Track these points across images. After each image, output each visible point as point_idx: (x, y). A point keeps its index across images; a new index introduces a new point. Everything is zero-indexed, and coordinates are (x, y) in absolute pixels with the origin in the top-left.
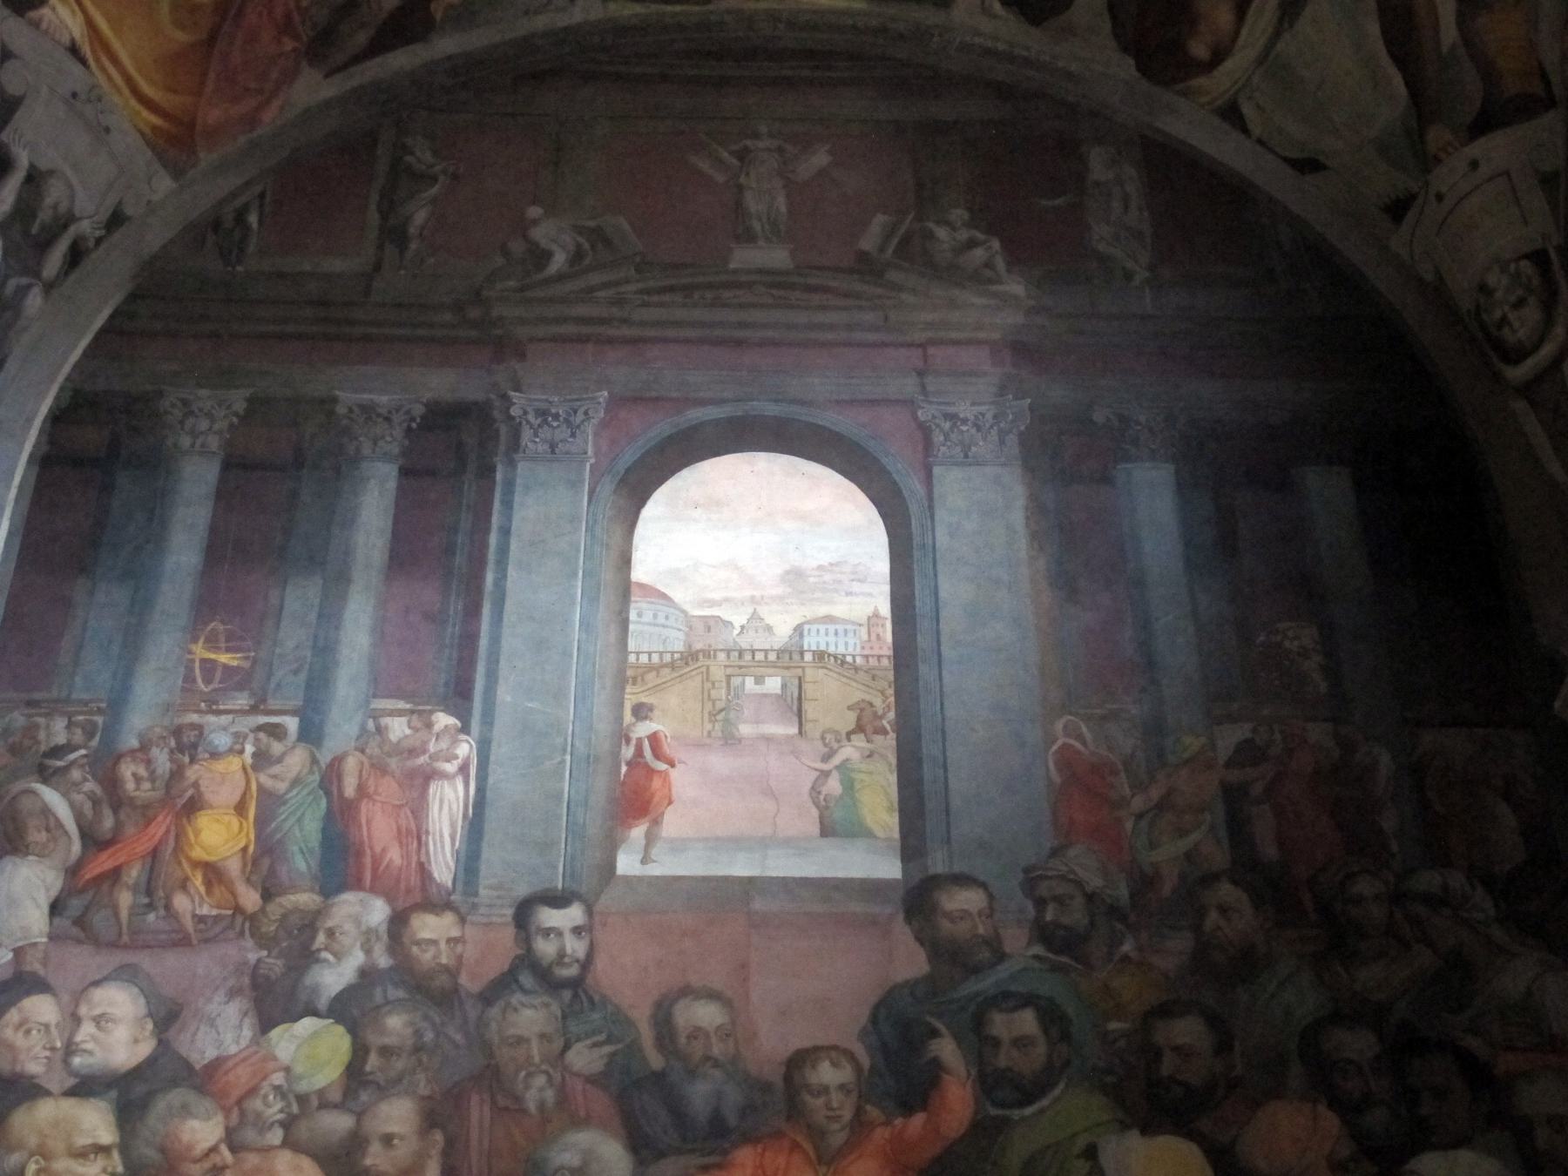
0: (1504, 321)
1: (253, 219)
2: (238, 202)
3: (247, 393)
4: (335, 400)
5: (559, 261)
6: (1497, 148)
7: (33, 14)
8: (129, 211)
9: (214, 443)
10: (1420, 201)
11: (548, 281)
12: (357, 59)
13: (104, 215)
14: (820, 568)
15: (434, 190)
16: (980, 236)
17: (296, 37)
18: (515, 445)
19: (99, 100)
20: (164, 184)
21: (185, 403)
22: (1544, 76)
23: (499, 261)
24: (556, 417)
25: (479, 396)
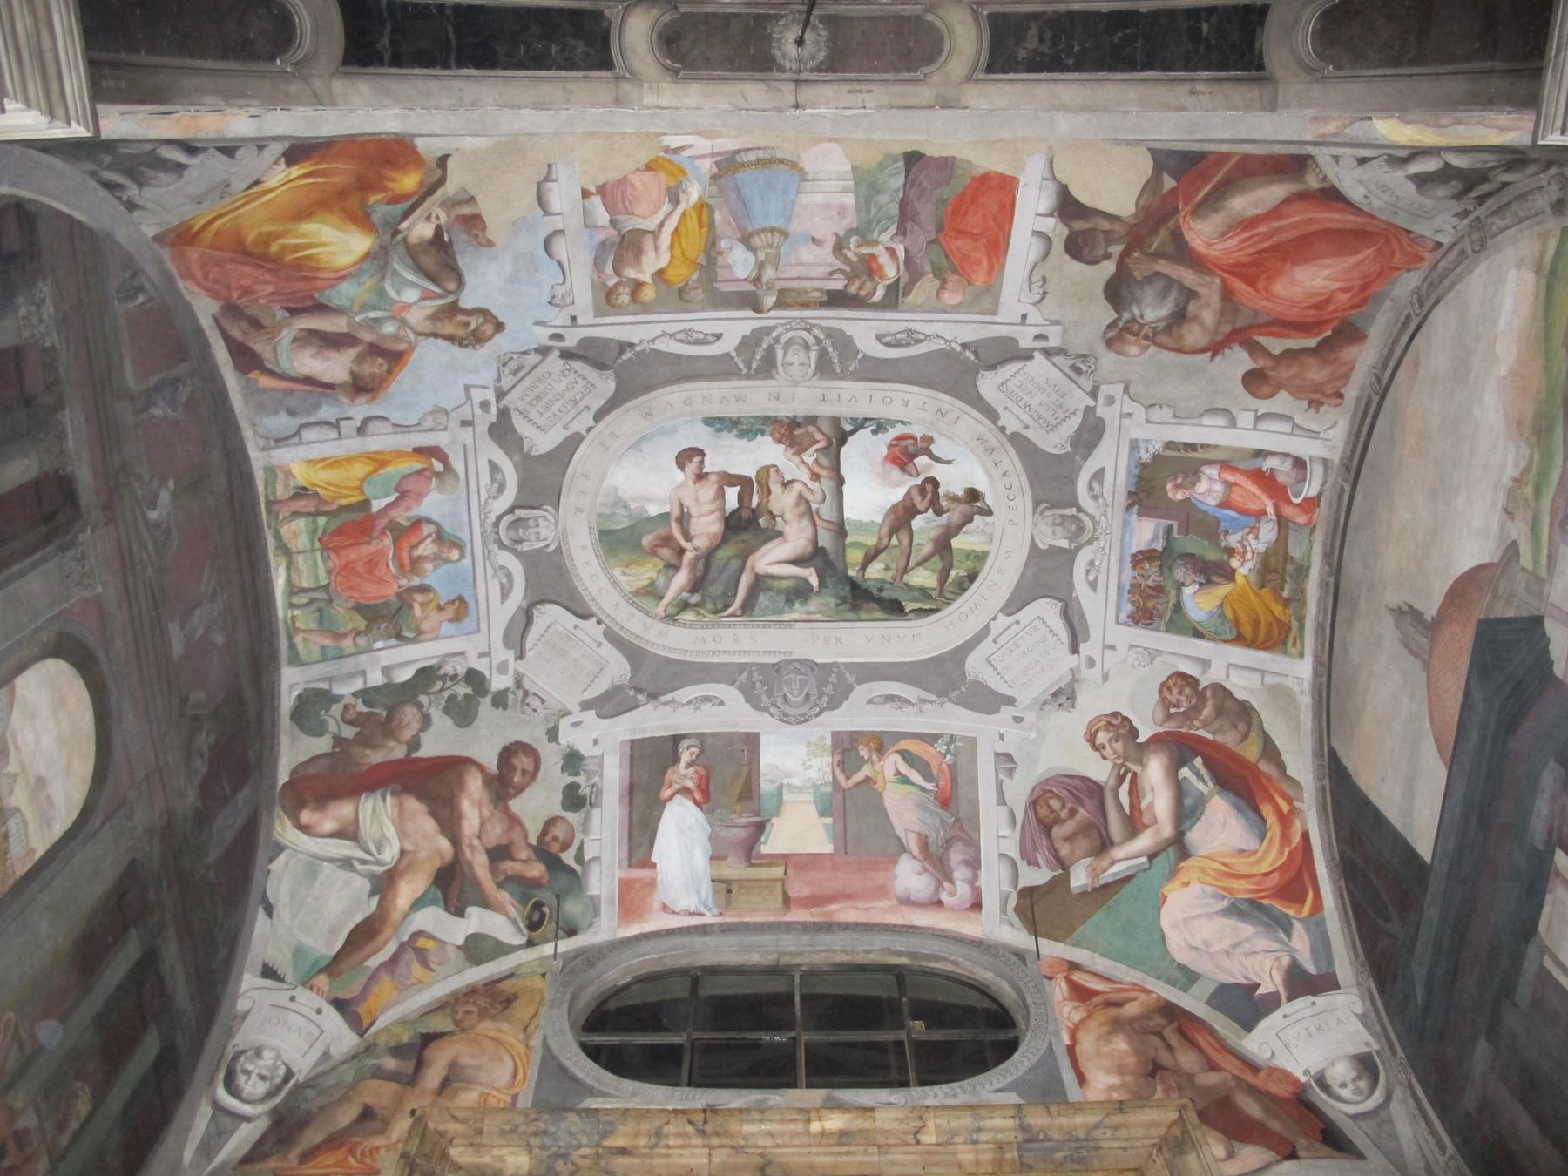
0: (247, 1073)
1: (141, 299)
2: (147, 286)
3: (57, 344)
4: (63, 409)
5: (153, 515)
6: (333, 1018)
7: (283, 160)
8: (136, 214)
9: (26, 334)
10: (285, 986)
11: (144, 514)
12: (220, 327)
13: (138, 200)
14: (48, 797)
15: (170, 412)
16: (206, 758)
17: (240, 297)
18: (63, 549)
19: (222, 198)
20: (150, 230)
21: (43, 300)
22: (372, 1024)
23: (147, 478)
24: (83, 567)
25: (83, 510)
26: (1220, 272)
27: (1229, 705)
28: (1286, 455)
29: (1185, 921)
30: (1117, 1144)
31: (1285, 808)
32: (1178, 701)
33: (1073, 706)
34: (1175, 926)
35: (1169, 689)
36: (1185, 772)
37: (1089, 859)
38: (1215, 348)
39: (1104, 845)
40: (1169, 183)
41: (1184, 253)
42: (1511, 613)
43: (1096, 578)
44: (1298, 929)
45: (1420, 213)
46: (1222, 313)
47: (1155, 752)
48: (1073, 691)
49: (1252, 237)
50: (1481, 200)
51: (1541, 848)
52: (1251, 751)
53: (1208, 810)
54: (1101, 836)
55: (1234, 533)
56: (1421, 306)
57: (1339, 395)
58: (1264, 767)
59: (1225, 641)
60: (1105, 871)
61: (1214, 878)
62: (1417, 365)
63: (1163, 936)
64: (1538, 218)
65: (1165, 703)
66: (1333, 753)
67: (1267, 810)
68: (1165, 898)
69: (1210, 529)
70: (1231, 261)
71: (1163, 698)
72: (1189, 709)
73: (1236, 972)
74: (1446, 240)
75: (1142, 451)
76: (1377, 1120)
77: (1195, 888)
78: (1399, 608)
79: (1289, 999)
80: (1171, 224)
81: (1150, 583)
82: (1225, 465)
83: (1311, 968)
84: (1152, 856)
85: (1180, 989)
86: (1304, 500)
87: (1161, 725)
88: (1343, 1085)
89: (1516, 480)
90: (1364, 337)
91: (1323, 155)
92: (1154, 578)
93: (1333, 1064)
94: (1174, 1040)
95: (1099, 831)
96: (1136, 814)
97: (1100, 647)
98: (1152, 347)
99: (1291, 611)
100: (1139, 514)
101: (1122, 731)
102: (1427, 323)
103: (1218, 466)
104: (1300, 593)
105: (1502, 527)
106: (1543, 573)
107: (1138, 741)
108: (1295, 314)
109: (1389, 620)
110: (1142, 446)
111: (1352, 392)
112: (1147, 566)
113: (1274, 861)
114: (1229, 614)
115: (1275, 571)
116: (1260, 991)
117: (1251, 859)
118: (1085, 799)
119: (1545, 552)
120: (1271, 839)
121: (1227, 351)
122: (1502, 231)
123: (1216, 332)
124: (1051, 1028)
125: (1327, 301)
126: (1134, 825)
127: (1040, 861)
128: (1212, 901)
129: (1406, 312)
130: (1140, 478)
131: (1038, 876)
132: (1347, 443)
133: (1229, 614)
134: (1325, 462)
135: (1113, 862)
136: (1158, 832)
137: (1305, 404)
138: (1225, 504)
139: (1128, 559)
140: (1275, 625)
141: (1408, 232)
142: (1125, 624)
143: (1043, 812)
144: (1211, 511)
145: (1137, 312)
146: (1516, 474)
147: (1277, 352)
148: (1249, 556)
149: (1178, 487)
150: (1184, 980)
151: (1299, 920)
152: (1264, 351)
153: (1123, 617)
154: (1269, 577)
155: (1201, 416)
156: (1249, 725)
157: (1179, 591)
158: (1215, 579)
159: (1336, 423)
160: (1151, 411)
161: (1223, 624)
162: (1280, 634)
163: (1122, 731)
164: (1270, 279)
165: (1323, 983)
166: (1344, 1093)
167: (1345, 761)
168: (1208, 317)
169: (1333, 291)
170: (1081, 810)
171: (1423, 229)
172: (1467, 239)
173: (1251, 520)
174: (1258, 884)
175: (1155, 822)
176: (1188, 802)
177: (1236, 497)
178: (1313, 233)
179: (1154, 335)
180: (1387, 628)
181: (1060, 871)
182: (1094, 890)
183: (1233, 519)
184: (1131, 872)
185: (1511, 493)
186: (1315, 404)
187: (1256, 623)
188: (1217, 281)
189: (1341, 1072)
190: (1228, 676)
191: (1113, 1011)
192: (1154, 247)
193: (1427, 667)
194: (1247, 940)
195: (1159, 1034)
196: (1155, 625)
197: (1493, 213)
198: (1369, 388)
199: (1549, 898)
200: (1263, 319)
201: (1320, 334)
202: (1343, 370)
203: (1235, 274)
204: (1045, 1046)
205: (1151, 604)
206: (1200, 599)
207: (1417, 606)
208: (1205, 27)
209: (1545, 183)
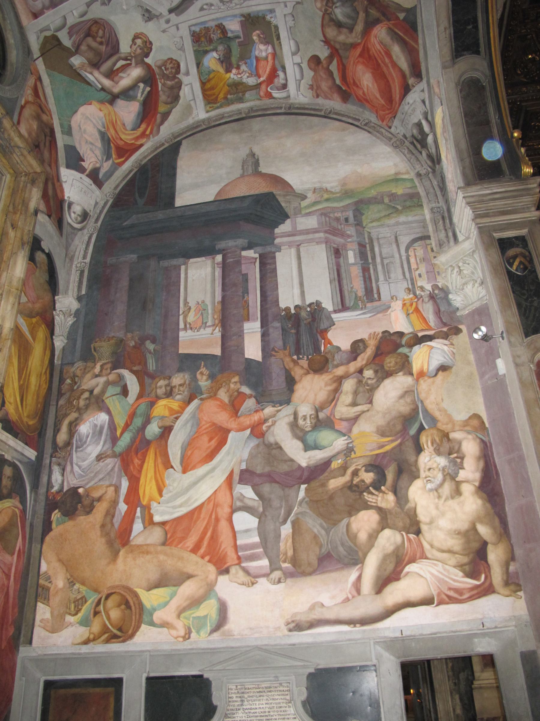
26: (363, 43)
27: (175, 91)
28: (286, 80)
29: (87, 118)
30: (17, 159)
31: (148, 132)
32: (168, 68)
33: (146, 21)
34: (83, 114)
35: (171, 62)
36: (142, 85)
37: (86, 61)
38: (327, 42)
39: (96, 65)
40: (402, 16)
41: (370, 25)
42: (283, 205)
43: (206, 9)
44: (110, 162)
45: (404, 123)
46: (344, 44)
47: (143, 69)
48: (152, 19)
49: (382, 55)
50: (412, 143)
51: (217, 249)
52: (162, 108)
53: (132, 103)
54: (99, 62)
55: (246, 67)
56: (365, 125)
57: (318, 96)
58: (159, 117)
59: (200, 78)
60: (86, 71)
61: (109, 120)
62: (343, 130)
63: (76, 112)
64: (412, 168)
65: (165, 63)
66: (179, 144)
67: (143, 126)
68: (91, 104)
69: (244, 56)
70: (370, 46)
71: (166, 61)
72: (167, 75)
73: (83, 150)
74: (393, 130)
75: (271, 15)
76: (73, 231)
77: (101, 114)
78: (254, 154)
79: (87, 176)
80: (382, 18)
81: (212, 35)
82: (274, 55)
83: (101, 176)
84: (103, 89)
85: (62, 131)
86: (270, 93)
87: (155, 66)
88: (74, 213)
89: (327, 189)
90: (345, 103)
91: (423, 84)
92: (215, 37)
93: (78, 205)
94: (47, 144)
95: (100, 60)
96: (116, 73)
97: (176, 23)
98: (321, 14)
99: (223, 101)
100: (241, 21)
101: (145, 50)
102: (361, 130)
103: (273, 52)
104: (231, 102)
105: (309, 190)
106: (303, 212)
107: (145, 59)
108: (349, 74)
109: (248, 152)
110: (273, 15)
111: (320, 101)
112: (219, 32)
113: (127, 139)
114: (212, 76)
115: (237, 89)
116: (82, 163)
117: (123, 130)
118: (110, 46)
119: (310, 210)
120: (134, 133)
121: (326, 47)
122: (404, 154)
123: (335, 42)
124: (22, 92)
125: (357, 86)
126: (111, 74)
127: (73, 39)
128: (100, 124)
129: (360, 118)
130: (258, 17)
131: (67, 42)
132: (299, 104)
133: (212, 76)
134: (289, 97)
135: (91, 73)
136: (113, 87)
137: (310, 83)
138: (258, 59)
139: (219, 22)
140: (214, 97)
141: (395, 117)
142: (190, 30)
143: (94, 29)
144: (253, 54)
145: (338, 4)
146: (329, 189)
147: (330, 68)
148: (239, 76)
149: (259, 36)
150: (66, 130)
151: (113, 161)
152: (330, 62)
153: (193, 28)
154: (234, 87)
155: (293, 39)
156: (171, 103)
157: (213, 50)
158: (224, 65)
159: (306, 97)
160: (290, 16)
161: (206, 74)
162: (212, 100)
163: (145, 50)
164: (363, 63)
165: (99, 183)
166: (73, 215)
167: (181, 150)
168: (342, 38)
169: (362, 89)
170: (104, 47)
171: (396, 122)
172: (396, 139)
173: (255, 73)
174: (117, 138)
175: (117, 83)
176: (131, 93)
177: (262, 63)
178: (388, 81)
179: (328, 14)
180: (244, 152)
181: (74, 50)
182: (75, 70)
183: (252, 65)
184: (92, 84)
185: (321, 189)
186: (311, 87)
187: (212, 88)
188: (359, 41)
189: (77, 209)
190: (186, 85)
191: (40, 111)
192: (371, 11)
193: (242, 176)
194: (96, 146)
195: (45, 136)
196: (195, 44)
197: (408, 148)
198: (325, 108)
199: (203, 258)
200: (344, 61)
201: (343, 84)
202: (329, 96)
203: (363, 50)
204: (16, 96)
205: (203, 39)
206: (213, 61)
207: (261, 162)
208: (470, 27)
209: (424, 167)
